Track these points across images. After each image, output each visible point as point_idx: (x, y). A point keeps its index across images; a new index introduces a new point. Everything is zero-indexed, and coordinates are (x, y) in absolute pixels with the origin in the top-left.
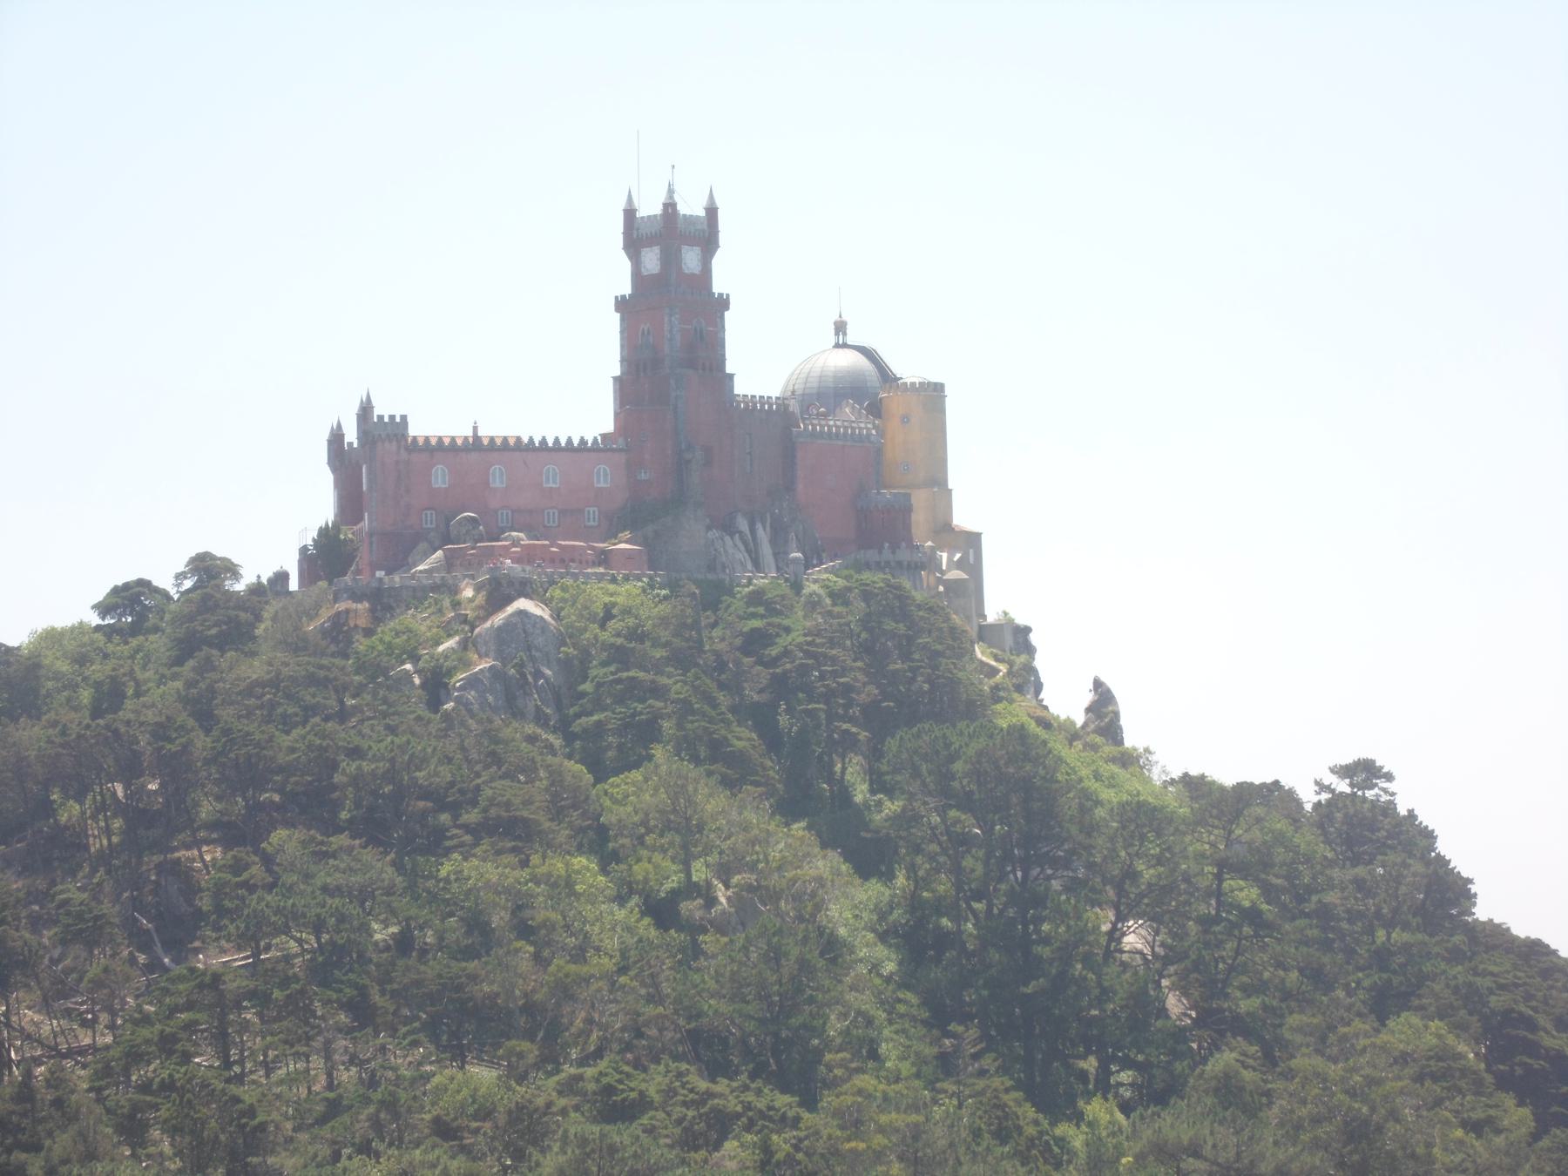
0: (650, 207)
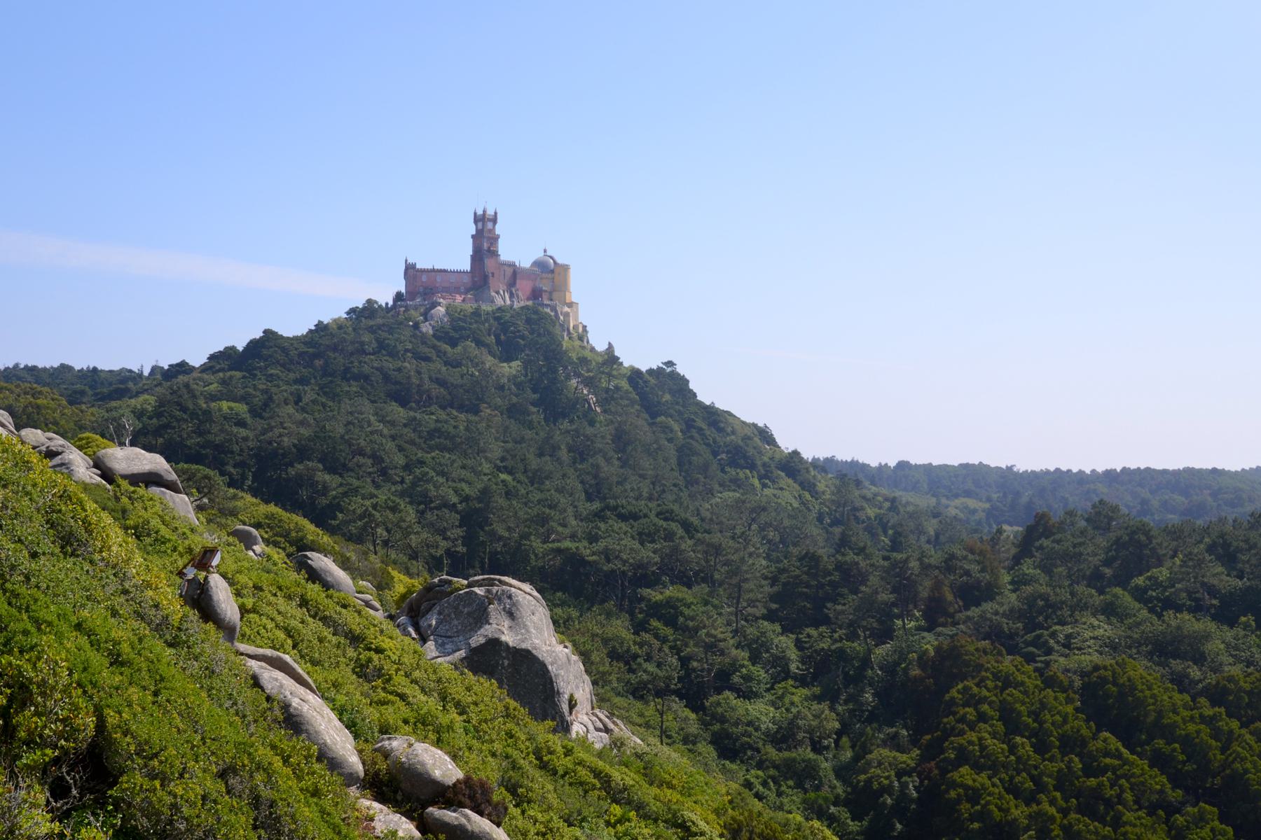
0: (480, 212)
